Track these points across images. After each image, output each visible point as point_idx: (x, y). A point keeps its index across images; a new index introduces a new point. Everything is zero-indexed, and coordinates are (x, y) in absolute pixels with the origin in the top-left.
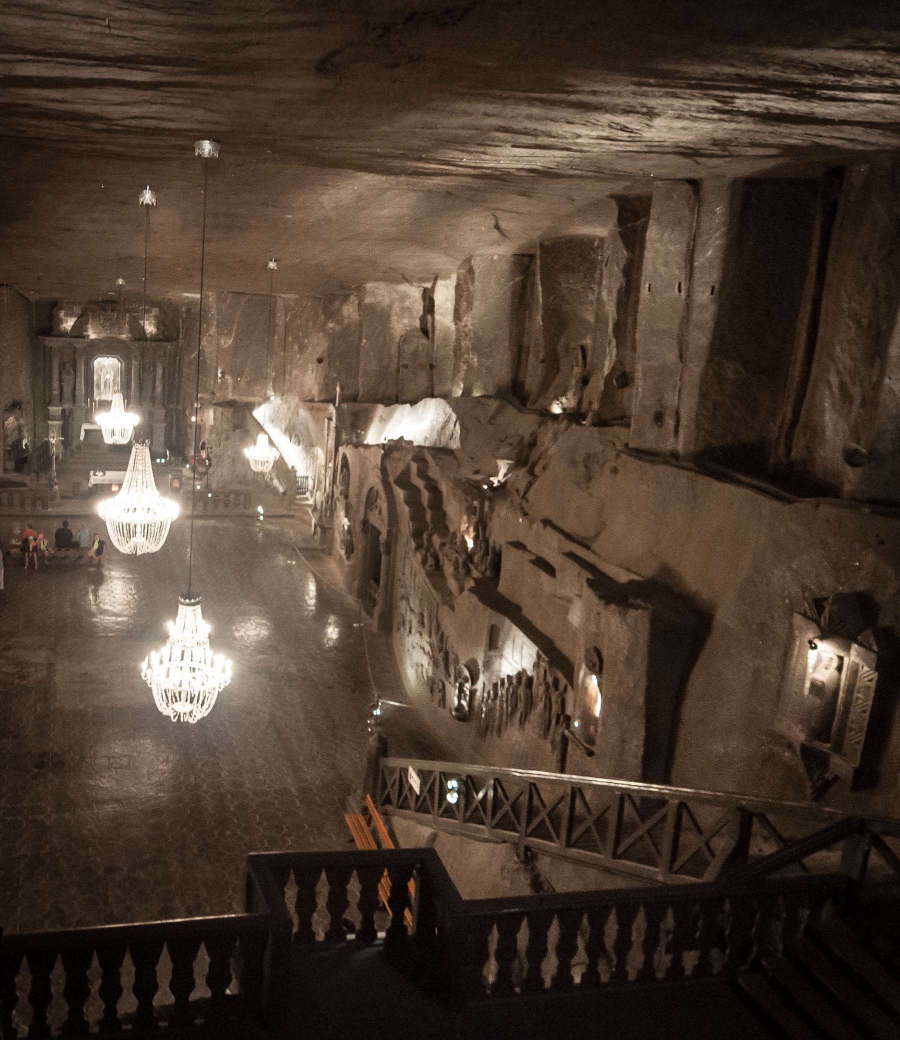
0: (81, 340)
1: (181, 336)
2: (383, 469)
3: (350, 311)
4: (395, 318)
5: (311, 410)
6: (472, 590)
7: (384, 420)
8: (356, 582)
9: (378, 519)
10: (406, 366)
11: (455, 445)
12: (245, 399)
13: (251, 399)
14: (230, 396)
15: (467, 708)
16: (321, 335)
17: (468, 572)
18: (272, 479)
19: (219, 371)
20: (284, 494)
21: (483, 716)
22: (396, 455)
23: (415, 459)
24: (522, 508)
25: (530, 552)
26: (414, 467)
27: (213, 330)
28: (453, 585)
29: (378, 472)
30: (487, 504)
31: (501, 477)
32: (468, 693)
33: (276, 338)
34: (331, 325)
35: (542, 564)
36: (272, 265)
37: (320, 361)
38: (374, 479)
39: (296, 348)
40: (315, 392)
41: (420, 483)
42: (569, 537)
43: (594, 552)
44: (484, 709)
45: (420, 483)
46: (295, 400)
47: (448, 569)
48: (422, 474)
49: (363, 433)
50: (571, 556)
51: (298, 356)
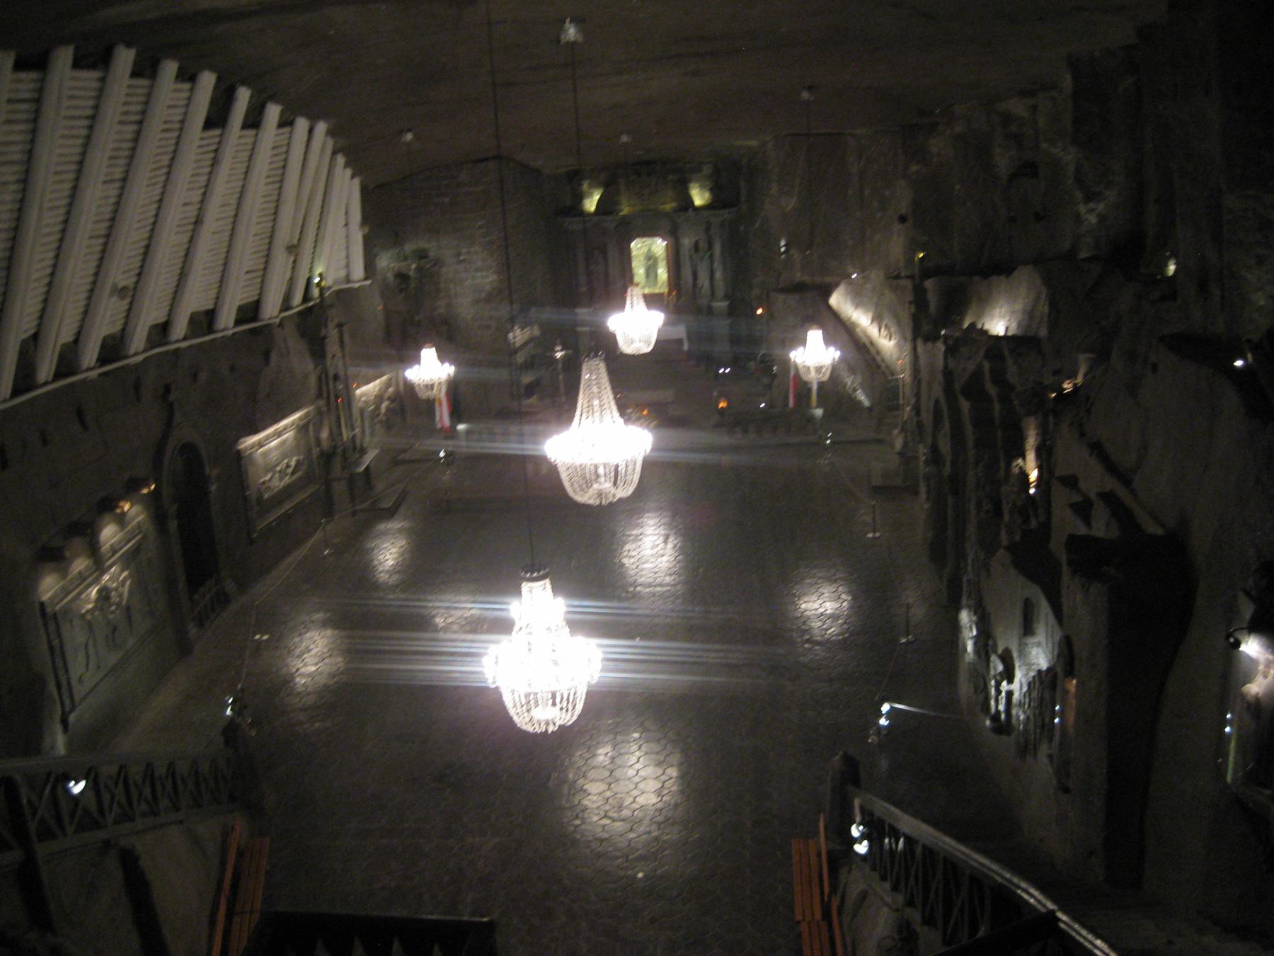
0: (610, 218)
1: (743, 199)
2: (948, 374)
3: (939, 146)
4: (998, 150)
5: (895, 289)
6: (1011, 548)
7: (985, 302)
8: (930, 535)
9: (945, 446)
10: (1012, 220)
11: (1043, 333)
12: (818, 279)
13: (828, 279)
14: (799, 277)
15: (1003, 716)
16: (902, 183)
17: (1026, 520)
18: (855, 390)
19: (783, 243)
20: (870, 409)
21: (1021, 727)
22: (964, 351)
23: (986, 356)
24: (1082, 425)
25: (1079, 491)
26: (987, 365)
27: (774, 189)
28: (1004, 539)
29: (940, 377)
30: (1051, 419)
31: (1079, 380)
32: (1003, 694)
33: (850, 192)
34: (914, 168)
35: (1083, 510)
36: (805, 95)
37: (903, 219)
38: (938, 391)
39: (876, 204)
40: (901, 264)
41: (992, 390)
42: (1111, 467)
43: (1133, 491)
44: (1022, 718)
45: (992, 390)
46: (877, 276)
47: (1006, 517)
48: (999, 379)
49: (958, 318)
50: (1108, 498)
51: (879, 215)
